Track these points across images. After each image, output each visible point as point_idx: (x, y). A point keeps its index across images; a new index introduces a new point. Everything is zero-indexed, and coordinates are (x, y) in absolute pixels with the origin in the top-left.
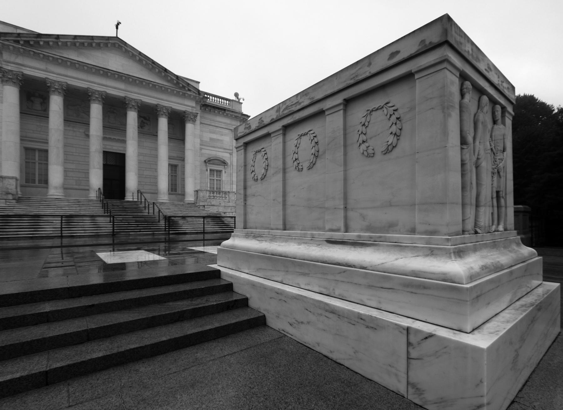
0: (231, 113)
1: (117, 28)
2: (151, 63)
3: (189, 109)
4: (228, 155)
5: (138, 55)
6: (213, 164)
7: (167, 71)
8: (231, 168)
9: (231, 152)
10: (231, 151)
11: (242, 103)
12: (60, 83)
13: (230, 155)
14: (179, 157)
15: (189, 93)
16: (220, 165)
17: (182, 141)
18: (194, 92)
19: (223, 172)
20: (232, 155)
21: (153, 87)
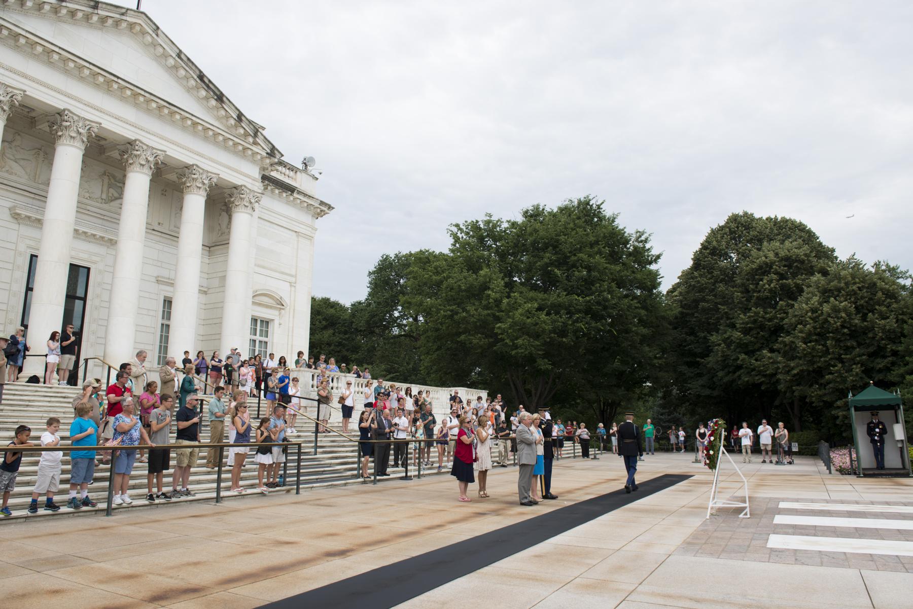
2: (196, 77)
5: (174, 56)
6: (260, 304)
7: (225, 99)
8: (291, 316)
9: (293, 280)
10: (293, 280)
11: (317, 179)
12: (9, 90)
13: (291, 286)
15: (255, 148)
16: (271, 307)
17: (208, 249)
18: (263, 149)
19: (276, 322)
21: (193, 126)
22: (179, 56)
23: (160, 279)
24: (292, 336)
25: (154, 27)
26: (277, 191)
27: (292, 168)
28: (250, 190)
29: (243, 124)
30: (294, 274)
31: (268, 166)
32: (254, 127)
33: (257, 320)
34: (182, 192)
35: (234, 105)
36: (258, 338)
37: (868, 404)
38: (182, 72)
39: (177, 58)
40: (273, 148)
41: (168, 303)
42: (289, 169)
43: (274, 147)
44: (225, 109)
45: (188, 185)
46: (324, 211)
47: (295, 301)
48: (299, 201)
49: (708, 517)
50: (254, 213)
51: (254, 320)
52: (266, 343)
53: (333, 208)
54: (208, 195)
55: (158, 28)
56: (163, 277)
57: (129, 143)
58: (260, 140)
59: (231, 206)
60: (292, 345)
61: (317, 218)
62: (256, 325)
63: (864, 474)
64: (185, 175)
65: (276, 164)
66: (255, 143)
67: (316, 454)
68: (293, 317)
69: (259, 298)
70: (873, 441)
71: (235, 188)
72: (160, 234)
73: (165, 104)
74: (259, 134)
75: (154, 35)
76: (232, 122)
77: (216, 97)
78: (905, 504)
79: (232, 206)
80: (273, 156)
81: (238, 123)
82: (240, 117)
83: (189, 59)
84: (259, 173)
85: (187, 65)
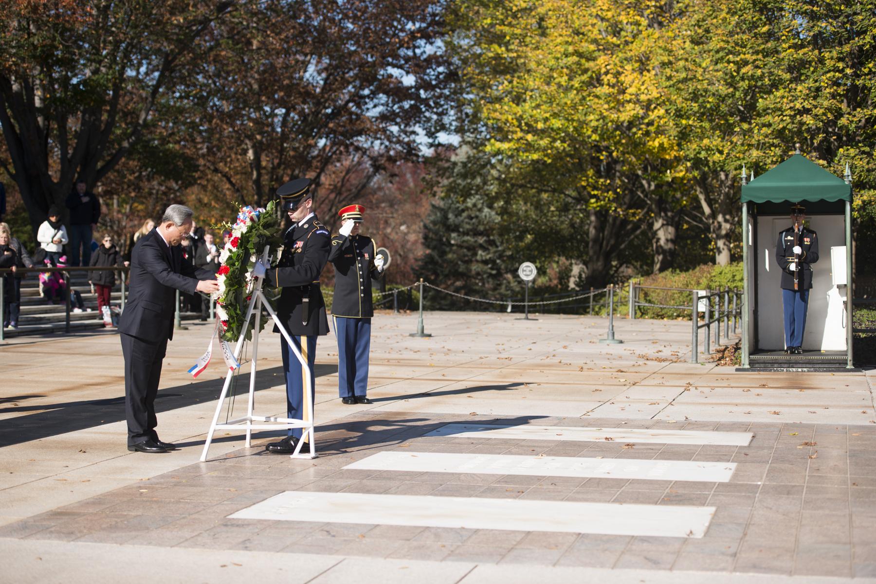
37: (777, 199)
49: (203, 458)
63: (750, 364)
78: (718, 427)
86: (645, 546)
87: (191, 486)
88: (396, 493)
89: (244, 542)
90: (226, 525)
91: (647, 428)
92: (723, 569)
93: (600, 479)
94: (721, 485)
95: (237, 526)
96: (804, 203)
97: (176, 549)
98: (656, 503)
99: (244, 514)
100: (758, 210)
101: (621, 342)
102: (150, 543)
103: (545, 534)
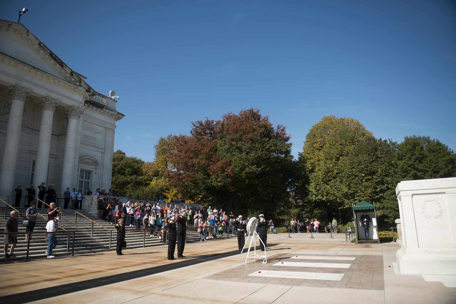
0: (107, 111)
1: (20, 15)
2: (48, 54)
3: (77, 104)
4: (99, 154)
6: (84, 163)
7: (64, 65)
9: (103, 151)
11: (117, 102)
13: (102, 154)
14: (53, 155)
15: (80, 88)
16: (91, 165)
17: (57, 137)
18: (84, 88)
20: (104, 154)
22: (40, 44)
23: (31, 152)
24: (102, 179)
25: (26, 31)
26: (94, 108)
27: (103, 96)
28: (78, 108)
29: (74, 77)
30: (103, 147)
31: (87, 96)
32: (79, 77)
33: (83, 171)
34: (42, 109)
35: (68, 67)
36: (84, 180)
38: (42, 51)
39: (38, 45)
40: (90, 88)
41: (34, 163)
42: (102, 97)
43: (90, 87)
44: (64, 69)
45: (45, 106)
46: (120, 117)
47: (104, 161)
48: (106, 112)
49: (245, 263)
50: (79, 119)
51: (82, 171)
52: (88, 182)
53: (125, 116)
54: (55, 111)
55: (28, 31)
56: (33, 151)
57: (13, 86)
58: (83, 84)
59: (68, 116)
60: (102, 183)
61: (117, 121)
62: (83, 174)
64: (43, 101)
65: (91, 95)
66: (80, 86)
67: (92, 237)
68: (103, 170)
69: (82, 159)
70: (363, 225)
71: (70, 107)
72: (31, 130)
73: (32, 67)
74: (82, 81)
75: (26, 34)
76: (68, 75)
77: (59, 64)
78: (349, 256)
79: (68, 116)
80: (90, 92)
81: (71, 76)
82: (72, 73)
83: (44, 46)
84: (83, 99)
85: (44, 48)
86: (328, 282)
87: (242, 269)
88: (281, 271)
89: (249, 281)
90: (246, 277)
91: (334, 256)
92: (343, 288)
93: (322, 268)
94: (347, 269)
95: (249, 277)
96: (366, 210)
97: (236, 282)
98: (332, 273)
99: (250, 275)
100: (357, 211)
101: (333, 238)
102: (231, 281)
103: (308, 280)
